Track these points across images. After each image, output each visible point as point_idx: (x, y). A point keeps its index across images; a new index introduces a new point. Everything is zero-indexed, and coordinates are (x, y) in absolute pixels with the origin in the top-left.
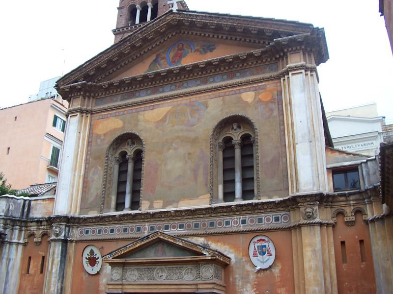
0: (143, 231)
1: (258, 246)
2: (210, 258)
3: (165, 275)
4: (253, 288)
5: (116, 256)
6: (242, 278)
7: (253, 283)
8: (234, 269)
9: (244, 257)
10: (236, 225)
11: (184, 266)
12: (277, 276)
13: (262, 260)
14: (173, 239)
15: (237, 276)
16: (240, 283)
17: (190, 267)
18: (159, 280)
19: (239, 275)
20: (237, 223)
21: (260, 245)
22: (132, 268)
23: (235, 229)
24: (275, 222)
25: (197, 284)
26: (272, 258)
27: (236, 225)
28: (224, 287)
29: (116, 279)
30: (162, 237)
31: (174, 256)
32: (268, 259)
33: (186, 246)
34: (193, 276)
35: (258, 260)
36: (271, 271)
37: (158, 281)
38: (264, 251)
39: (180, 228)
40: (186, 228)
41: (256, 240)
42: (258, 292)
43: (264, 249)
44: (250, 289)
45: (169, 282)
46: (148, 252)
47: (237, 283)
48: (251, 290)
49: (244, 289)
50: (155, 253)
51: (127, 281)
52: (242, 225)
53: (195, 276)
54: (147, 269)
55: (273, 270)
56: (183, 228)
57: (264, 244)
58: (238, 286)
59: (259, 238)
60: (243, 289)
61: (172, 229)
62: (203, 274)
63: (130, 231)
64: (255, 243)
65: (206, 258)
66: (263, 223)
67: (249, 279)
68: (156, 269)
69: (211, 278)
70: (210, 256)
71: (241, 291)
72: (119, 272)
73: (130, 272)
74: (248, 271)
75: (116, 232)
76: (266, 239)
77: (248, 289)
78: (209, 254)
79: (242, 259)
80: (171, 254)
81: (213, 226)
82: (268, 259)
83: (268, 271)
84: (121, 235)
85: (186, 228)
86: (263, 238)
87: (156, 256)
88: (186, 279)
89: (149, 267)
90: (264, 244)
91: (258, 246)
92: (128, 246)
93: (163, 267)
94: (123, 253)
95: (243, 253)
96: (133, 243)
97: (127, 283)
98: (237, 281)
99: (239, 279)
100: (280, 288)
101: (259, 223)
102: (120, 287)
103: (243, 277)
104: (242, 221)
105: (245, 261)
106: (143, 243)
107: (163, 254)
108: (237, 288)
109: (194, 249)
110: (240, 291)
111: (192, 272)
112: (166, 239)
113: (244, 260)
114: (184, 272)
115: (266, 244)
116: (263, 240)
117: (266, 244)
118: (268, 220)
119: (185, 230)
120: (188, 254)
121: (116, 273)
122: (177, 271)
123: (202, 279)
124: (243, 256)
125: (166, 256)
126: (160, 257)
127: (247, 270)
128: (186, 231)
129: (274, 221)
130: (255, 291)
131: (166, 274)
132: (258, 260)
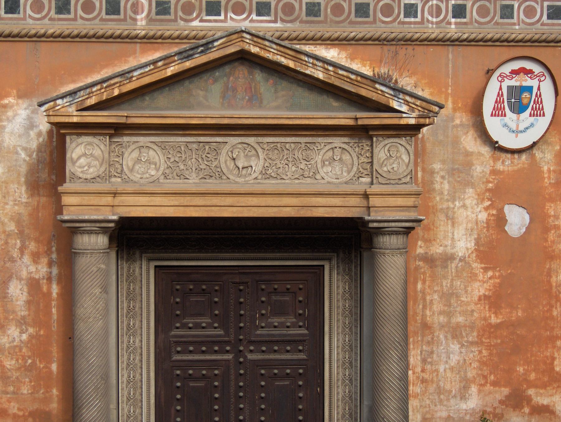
0: (129, 12)
1: (510, 88)
2: (412, 121)
3: (258, 165)
4: (483, 200)
5: (92, 101)
6: (452, 172)
7: (483, 187)
8: (428, 146)
9: (458, 114)
10: (435, 20)
11: (320, 139)
12: (549, 171)
13: (514, 129)
14: (295, 59)
15: (437, 166)
16: (446, 186)
17: (338, 141)
18: (238, 180)
19: (443, 162)
20: (438, 15)
21: (518, 84)
22: (143, 140)
23: (432, 31)
24: (550, 21)
25: (366, 196)
26: (543, 123)
27: (435, 20)
28: (418, 194)
29: (89, 177)
30: (254, 50)
31: (291, 108)
32: (532, 125)
33: (338, 83)
34: (349, 172)
35: (505, 125)
36: (533, 156)
37: (237, 183)
38: (525, 101)
39: (259, 14)
40: (280, 14)
41: (507, 69)
42: (494, 212)
43: (526, 95)
44: (475, 202)
45: (271, 185)
46: (201, 93)
47: (437, 186)
48: (477, 204)
49: (457, 203)
50: (223, 97)
51: (127, 181)
52: (453, 20)
53: (355, 169)
54: (195, 146)
55: (538, 154)
56: (268, 14)
57: (528, 82)
58: (442, 193)
59: (516, 65)
60: (454, 201)
61: (230, 14)
62: (381, 166)
63: (80, 12)
64: (502, 77)
65: (403, 122)
66: (515, 20)
67: (472, 177)
68: (227, 147)
69: (408, 179)
70: (414, 115)
71: (448, 208)
72: (97, 152)
73: (135, 154)
74: (468, 154)
75: (29, 11)
76: (537, 69)
77: (468, 202)
78: (412, 110)
79: (453, 119)
80: (280, 101)
81: (368, 16)
82: (532, 125)
83: (524, 157)
84: (46, 21)
85: (280, 14)
86: (528, 65)
87: (231, 106)
88: (327, 179)
89: (202, 139)
90: (528, 82)
91: (510, 88)
92: (135, 74)
93: (251, 140)
94: (116, 92)
95: (453, 103)
96: (154, 62)
97: (130, 188)
98: (438, 179)
99: (442, 173)
100: (551, 200)
101: (502, 17)
102: (109, 200)
103: (453, 169)
104: (454, 6)
105: (462, 125)
106: (188, 64)
107: (250, 100)
108: (438, 199)
109: (363, 92)
110: (444, 206)
111: (346, 157)
112: (270, 56)
113: (458, 122)
114: (319, 158)
115: (534, 83)
116: (528, 72)
117: (534, 83)
118: (529, 12)
119: (275, 21)
120: (335, 104)
121: (85, 155)
122: (298, 154)
123: (381, 180)
124: (455, 110)
125: (260, 106)
126: (242, 108)
127: (466, 151)
128: (279, 25)
129: (545, 17)
130: (486, 209)
131: (262, 162)
132: (505, 125)
